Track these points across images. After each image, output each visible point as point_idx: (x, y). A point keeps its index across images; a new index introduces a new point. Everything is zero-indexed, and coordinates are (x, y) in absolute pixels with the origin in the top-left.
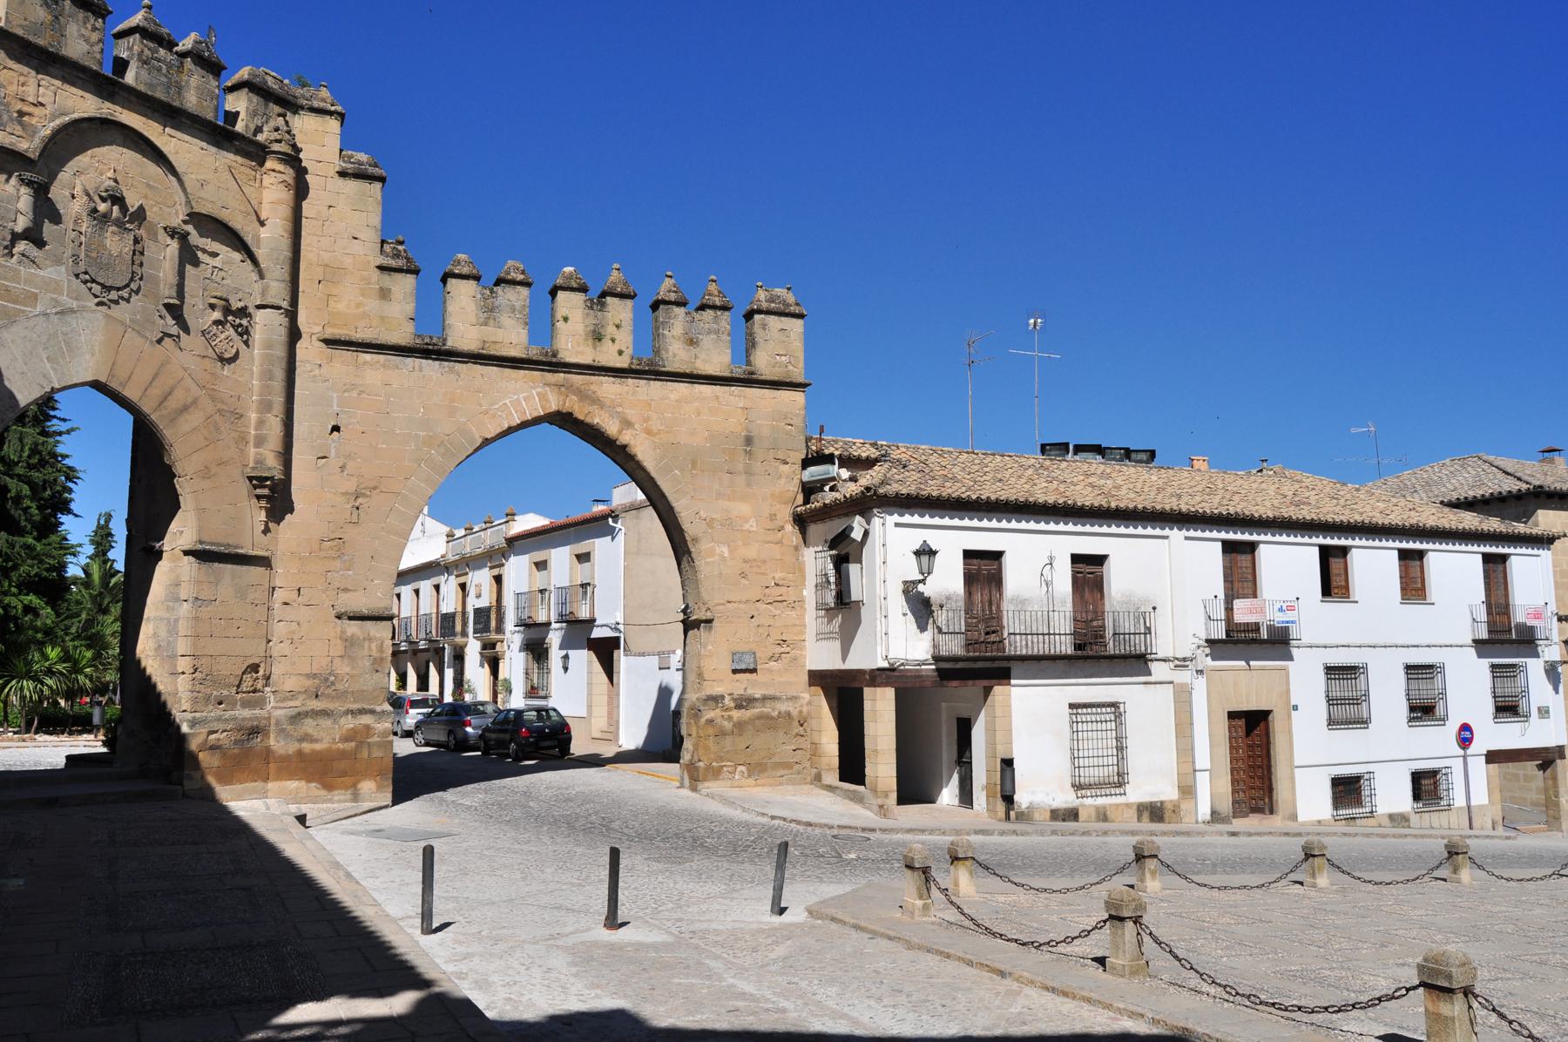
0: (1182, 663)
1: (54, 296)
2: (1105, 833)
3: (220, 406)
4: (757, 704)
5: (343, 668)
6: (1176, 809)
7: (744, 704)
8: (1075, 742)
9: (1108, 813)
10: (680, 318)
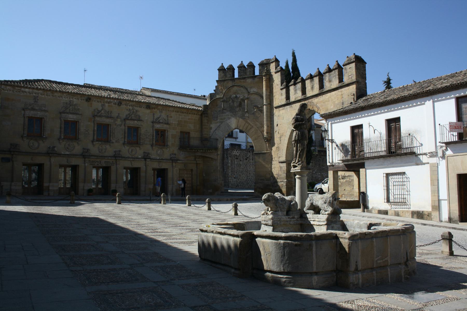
0: (433, 155)
1: (228, 117)
2: (371, 217)
3: (258, 126)
4: (346, 178)
5: (280, 173)
6: (429, 215)
7: (343, 178)
8: (404, 188)
9: (400, 213)
10: (328, 76)
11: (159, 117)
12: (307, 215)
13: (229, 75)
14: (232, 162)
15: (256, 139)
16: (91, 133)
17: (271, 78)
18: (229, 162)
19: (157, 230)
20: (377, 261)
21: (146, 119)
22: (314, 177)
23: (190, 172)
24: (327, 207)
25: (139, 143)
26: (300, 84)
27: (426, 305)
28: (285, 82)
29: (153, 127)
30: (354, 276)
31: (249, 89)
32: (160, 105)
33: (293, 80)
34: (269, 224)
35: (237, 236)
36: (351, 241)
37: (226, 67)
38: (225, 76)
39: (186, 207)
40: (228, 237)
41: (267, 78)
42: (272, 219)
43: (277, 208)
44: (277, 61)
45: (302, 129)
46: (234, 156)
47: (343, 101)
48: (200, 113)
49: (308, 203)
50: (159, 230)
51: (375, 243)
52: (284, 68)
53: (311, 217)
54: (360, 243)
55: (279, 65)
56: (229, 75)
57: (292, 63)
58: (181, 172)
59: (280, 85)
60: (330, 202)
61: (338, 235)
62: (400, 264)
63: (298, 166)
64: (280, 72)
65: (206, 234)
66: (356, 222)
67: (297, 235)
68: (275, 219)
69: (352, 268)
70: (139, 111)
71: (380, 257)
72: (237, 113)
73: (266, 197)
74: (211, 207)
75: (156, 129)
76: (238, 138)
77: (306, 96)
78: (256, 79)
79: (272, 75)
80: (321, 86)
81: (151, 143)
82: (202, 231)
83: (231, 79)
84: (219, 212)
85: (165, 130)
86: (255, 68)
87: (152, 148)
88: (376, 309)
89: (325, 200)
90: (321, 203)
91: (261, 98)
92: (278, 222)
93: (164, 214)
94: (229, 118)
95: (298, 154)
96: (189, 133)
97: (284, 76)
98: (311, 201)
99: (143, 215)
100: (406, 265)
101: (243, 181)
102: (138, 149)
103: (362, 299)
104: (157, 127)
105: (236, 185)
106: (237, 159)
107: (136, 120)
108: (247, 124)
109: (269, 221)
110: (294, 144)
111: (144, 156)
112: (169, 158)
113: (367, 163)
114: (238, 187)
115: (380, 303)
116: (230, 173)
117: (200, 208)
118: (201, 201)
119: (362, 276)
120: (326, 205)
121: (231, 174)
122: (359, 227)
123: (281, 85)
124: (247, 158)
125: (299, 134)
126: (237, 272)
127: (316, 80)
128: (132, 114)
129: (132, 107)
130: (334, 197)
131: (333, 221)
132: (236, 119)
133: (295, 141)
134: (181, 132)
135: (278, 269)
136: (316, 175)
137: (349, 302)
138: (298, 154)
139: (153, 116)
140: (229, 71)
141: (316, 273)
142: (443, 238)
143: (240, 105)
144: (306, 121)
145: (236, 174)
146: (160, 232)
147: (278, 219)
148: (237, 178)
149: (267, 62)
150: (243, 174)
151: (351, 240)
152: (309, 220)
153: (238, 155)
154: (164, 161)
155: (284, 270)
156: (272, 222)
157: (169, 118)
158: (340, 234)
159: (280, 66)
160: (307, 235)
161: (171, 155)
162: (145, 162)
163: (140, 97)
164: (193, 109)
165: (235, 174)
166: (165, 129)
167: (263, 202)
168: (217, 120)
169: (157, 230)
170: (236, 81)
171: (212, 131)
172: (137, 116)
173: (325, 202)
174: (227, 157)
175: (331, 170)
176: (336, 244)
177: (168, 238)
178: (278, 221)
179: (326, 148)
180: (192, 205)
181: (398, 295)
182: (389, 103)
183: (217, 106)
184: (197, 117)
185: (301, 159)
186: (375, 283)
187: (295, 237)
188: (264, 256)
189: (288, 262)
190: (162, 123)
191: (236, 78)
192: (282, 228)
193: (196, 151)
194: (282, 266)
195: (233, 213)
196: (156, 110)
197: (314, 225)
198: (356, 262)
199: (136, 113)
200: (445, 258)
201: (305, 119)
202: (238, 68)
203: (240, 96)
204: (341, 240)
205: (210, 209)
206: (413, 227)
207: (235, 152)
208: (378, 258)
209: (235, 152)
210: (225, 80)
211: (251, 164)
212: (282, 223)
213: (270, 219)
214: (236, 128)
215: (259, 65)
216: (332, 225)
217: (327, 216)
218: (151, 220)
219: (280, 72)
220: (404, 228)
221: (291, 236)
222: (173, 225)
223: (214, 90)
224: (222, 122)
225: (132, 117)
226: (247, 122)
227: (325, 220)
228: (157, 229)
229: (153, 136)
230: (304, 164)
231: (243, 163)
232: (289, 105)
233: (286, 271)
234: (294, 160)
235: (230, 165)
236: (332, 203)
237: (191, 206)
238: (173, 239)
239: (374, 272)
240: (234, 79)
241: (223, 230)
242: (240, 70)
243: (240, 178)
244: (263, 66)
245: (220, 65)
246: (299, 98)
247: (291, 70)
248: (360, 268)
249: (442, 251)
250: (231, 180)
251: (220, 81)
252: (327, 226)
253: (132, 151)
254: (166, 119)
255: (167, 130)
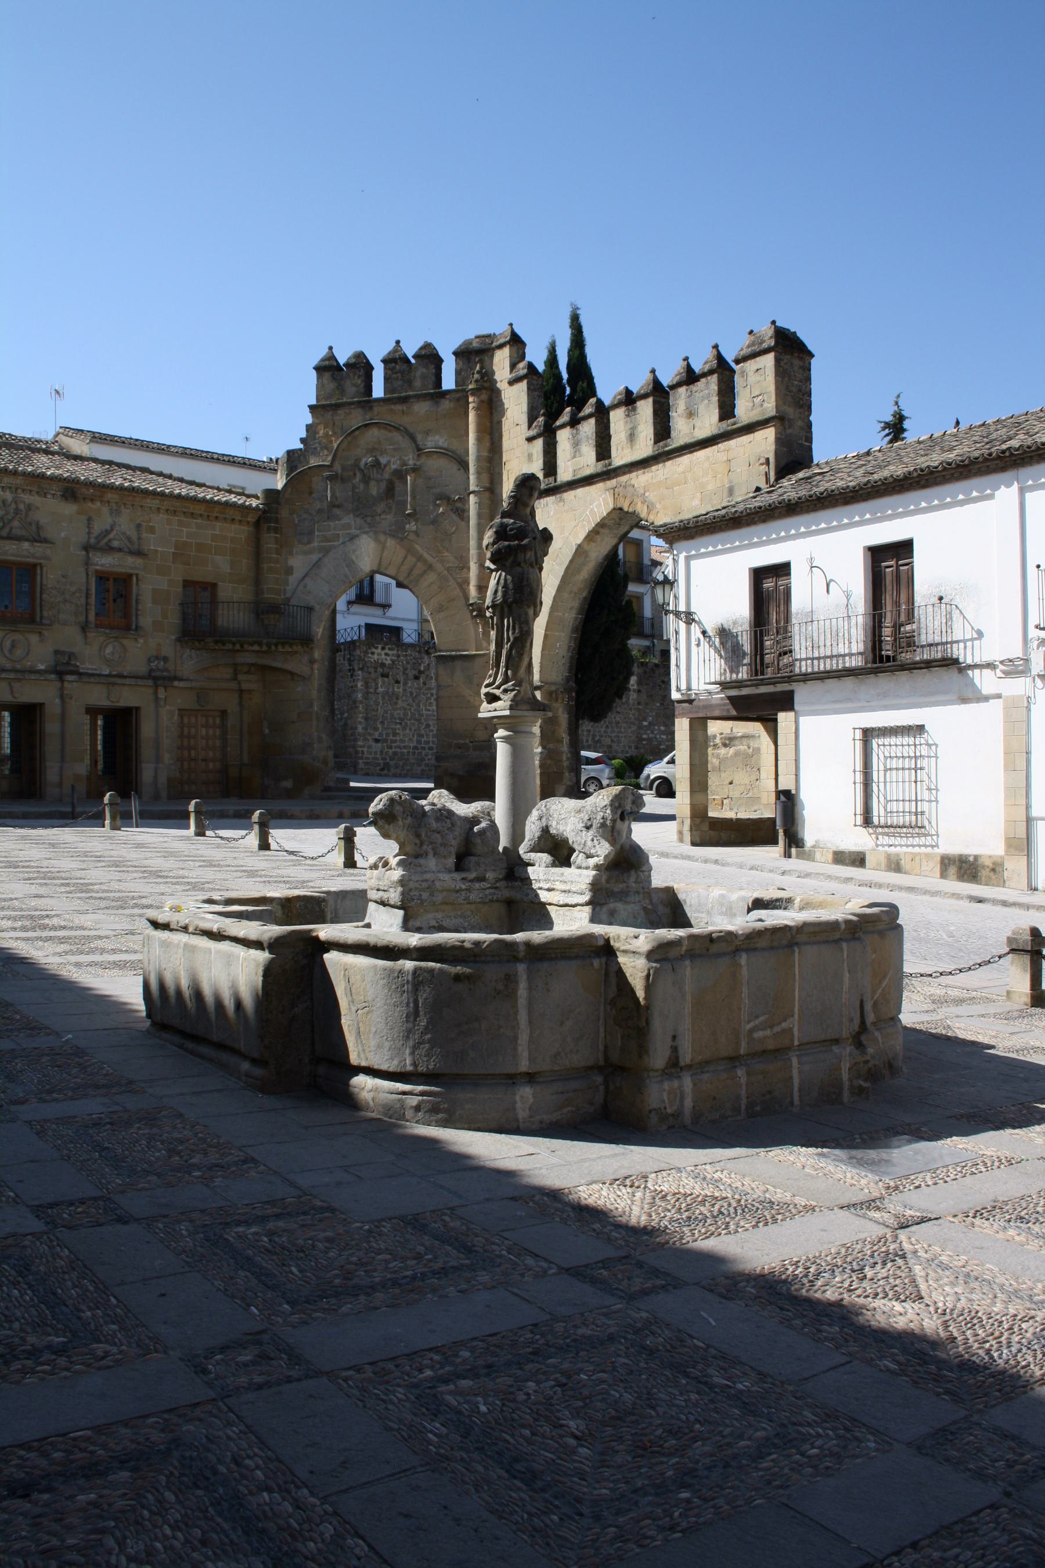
4: (736, 742)
10: (683, 396)
11: (108, 527)
12: (530, 869)
13: (352, 387)
14: (366, 684)
15: (440, 609)
17: (495, 399)
18: (356, 686)
19: (46, 921)
20: (751, 1031)
21: (63, 535)
22: (644, 739)
23: (218, 721)
24: (593, 840)
25: (38, 619)
26: (592, 421)
27: (896, 1188)
28: (543, 415)
29: (87, 563)
30: (666, 1085)
31: (419, 438)
32: (112, 487)
33: (568, 409)
34: (392, 903)
35: (257, 945)
36: (654, 965)
37: (342, 359)
38: (342, 391)
39: (188, 838)
40: (233, 949)
41: (482, 402)
42: (402, 882)
43: (422, 844)
44: (516, 341)
45: (519, 564)
46: (376, 668)
47: (730, 482)
48: (251, 519)
49: (532, 828)
50: (55, 921)
51: (744, 971)
52: (541, 367)
53: (541, 877)
54: (688, 970)
55: (523, 357)
56: (354, 389)
57: (570, 351)
58: (186, 720)
59: (525, 426)
60: (603, 825)
61: (612, 943)
62: (836, 1041)
63: (502, 696)
64: (525, 382)
65: (165, 935)
66: (716, 892)
67: (463, 942)
68: (412, 885)
69: (658, 1058)
70: (38, 508)
71: (762, 1018)
72: (377, 518)
73: (380, 807)
74: (270, 840)
75: (97, 571)
76: (390, 606)
77: (610, 464)
78: (446, 404)
79: (498, 392)
80: (662, 429)
81: (82, 619)
82: (156, 925)
83: (359, 402)
84: (294, 858)
85: (130, 576)
86: (444, 366)
87: (86, 637)
88: (717, 1207)
89: (587, 817)
90: (573, 827)
91: (462, 471)
92: (425, 895)
93: (100, 864)
94: (353, 538)
95: (504, 652)
96: (214, 586)
97: (539, 396)
98: (544, 820)
99: (23, 867)
100: (859, 1045)
101: (405, 751)
102: (34, 639)
103: (679, 1170)
104: (102, 565)
105: (379, 764)
106: (384, 675)
107: (27, 540)
108: (411, 559)
109: (391, 890)
110: (492, 618)
111: (56, 666)
112: (143, 670)
113: (802, 693)
114: (389, 770)
115: (739, 1184)
116: (360, 723)
117: (233, 844)
118: (239, 818)
119: (695, 1085)
120: (591, 832)
121: (365, 729)
122: (724, 909)
123: (530, 427)
124: (420, 672)
125: (509, 581)
126: (258, 1072)
127: (646, 409)
128: (13, 518)
129: (12, 492)
130: (620, 806)
131: (616, 890)
132: (377, 540)
133: (494, 606)
134: (187, 584)
135: (395, 1062)
136: (652, 732)
137: (628, 1182)
138: (504, 652)
139: (88, 527)
140: (355, 374)
141: (530, 1078)
142: (1014, 947)
143: (390, 491)
144: (534, 538)
145: (380, 726)
146: (54, 928)
147: (424, 885)
148: (386, 741)
149: (483, 347)
150: (404, 729)
151: (656, 961)
152: (535, 886)
153: (388, 662)
154: (128, 681)
155: (415, 1064)
156: (403, 894)
157: (144, 535)
158: (619, 937)
159: (528, 358)
160: (496, 941)
161: (149, 661)
162: (58, 684)
163: (44, 459)
164: (227, 503)
165: (376, 729)
166: (131, 571)
167: (370, 824)
168: (309, 542)
169: (46, 921)
170: (376, 409)
171: (293, 579)
172: (30, 524)
173: (589, 823)
174: (352, 670)
175: (683, 715)
176: (607, 974)
177: (72, 947)
178: (423, 890)
179: (668, 641)
180: (208, 833)
181: (812, 1150)
182: (877, 491)
183: (311, 493)
184: (241, 532)
185: (515, 674)
186: (743, 1107)
187: (454, 948)
188: (348, 1017)
189: (429, 1036)
190: (120, 550)
191: (378, 400)
192: (440, 915)
193: (238, 647)
194: (408, 1051)
195: (340, 860)
196: (98, 504)
197: (550, 904)
198: (674, 1037)
199: (27, 516)
200: (1015, 1014)
201: (533, 531)
202: (382, 365)
203: (389, 462)
204: (622, 959)
205: (264, 845)
206: (892, 910)
207: (379, 654)
208: (757, 1022)
209: (379, 654)
210: (337, 406)
211: (432, 695)
212: (439, 898)
213: (394, 884)
214: (375, 568)
215: (455, 353)
216: (612, 906)
217: (594, 872)
218: (41, 885)
219: (525, 382)
220: (855, 918)
221: (440, 945)
222: (114, 904)
223: (302, 440)
224: (326, 551)
225: (11, 528)
226: (410, 551)
227: (584, 887)
228: (47, 916)
229: (88, 596)
230: (522, 689)
231: (405, 690)
232: (553, 495)
233: (421, 1069)
234: (490, 676)
235: (360, 695)
236: (613, 827)
237: (204, 835)
238: (91, 951)
239: (740, 1072)
240: (369, 402)
241: (215, 924)
242: (389, 372)
243: (395, 741)
244: (469, 360)
245: (323, 352)
246: (588, 472)
247: (565, 376)
248: (686, 1056)
249: (1008, 992)
250: (363, 746)
251: (323, 407)
252: (593, 910)
253: (13, 646)
254: (134, 537)
255: (137, 575)
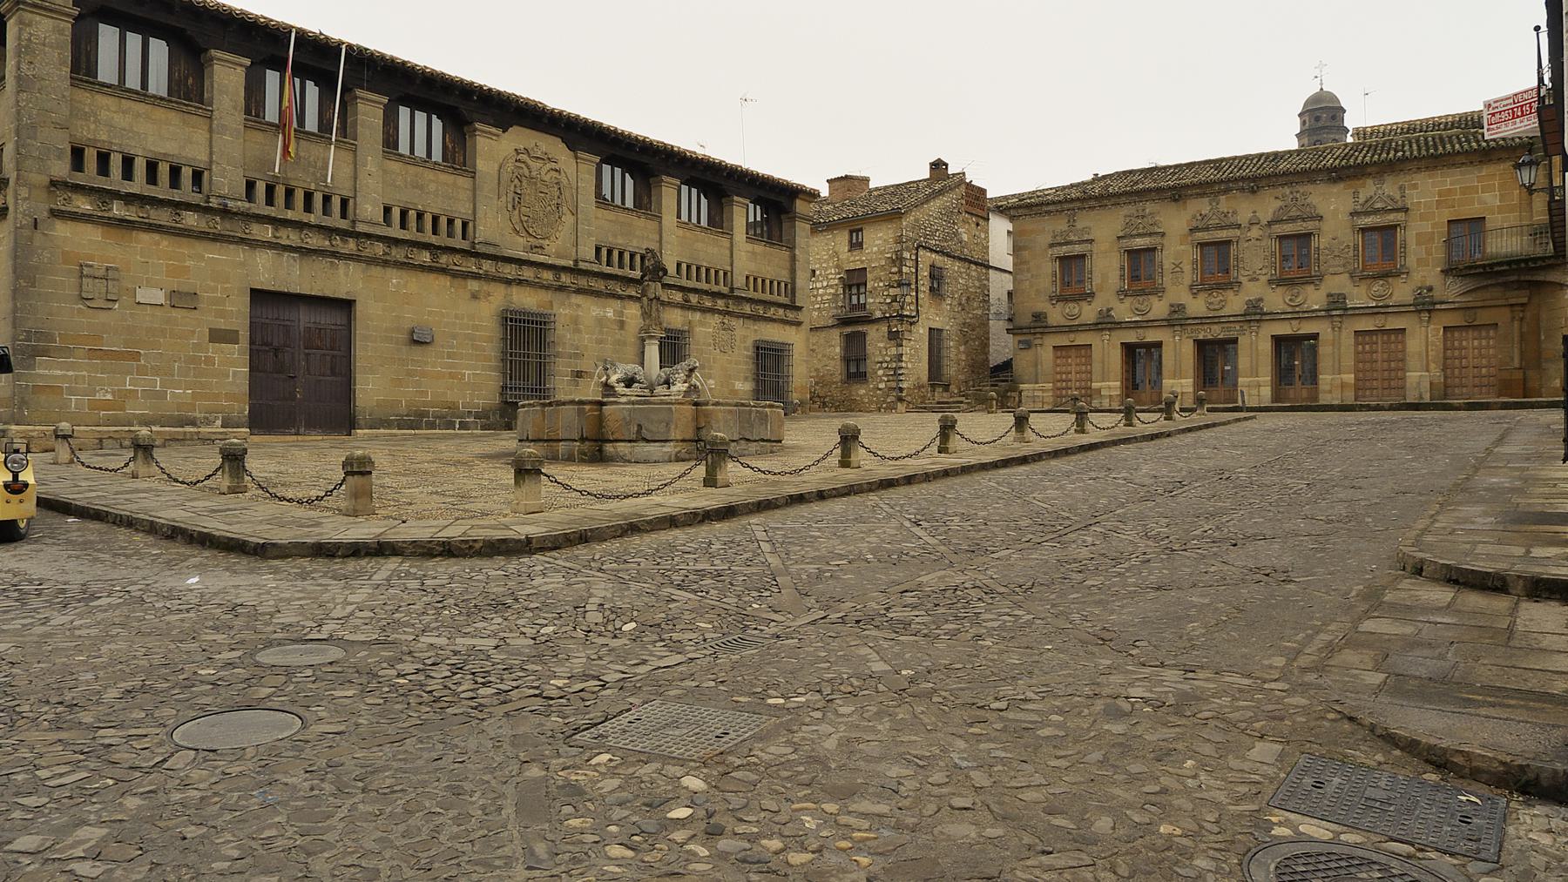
16: (1187, 268)
254: (1398, 197)
